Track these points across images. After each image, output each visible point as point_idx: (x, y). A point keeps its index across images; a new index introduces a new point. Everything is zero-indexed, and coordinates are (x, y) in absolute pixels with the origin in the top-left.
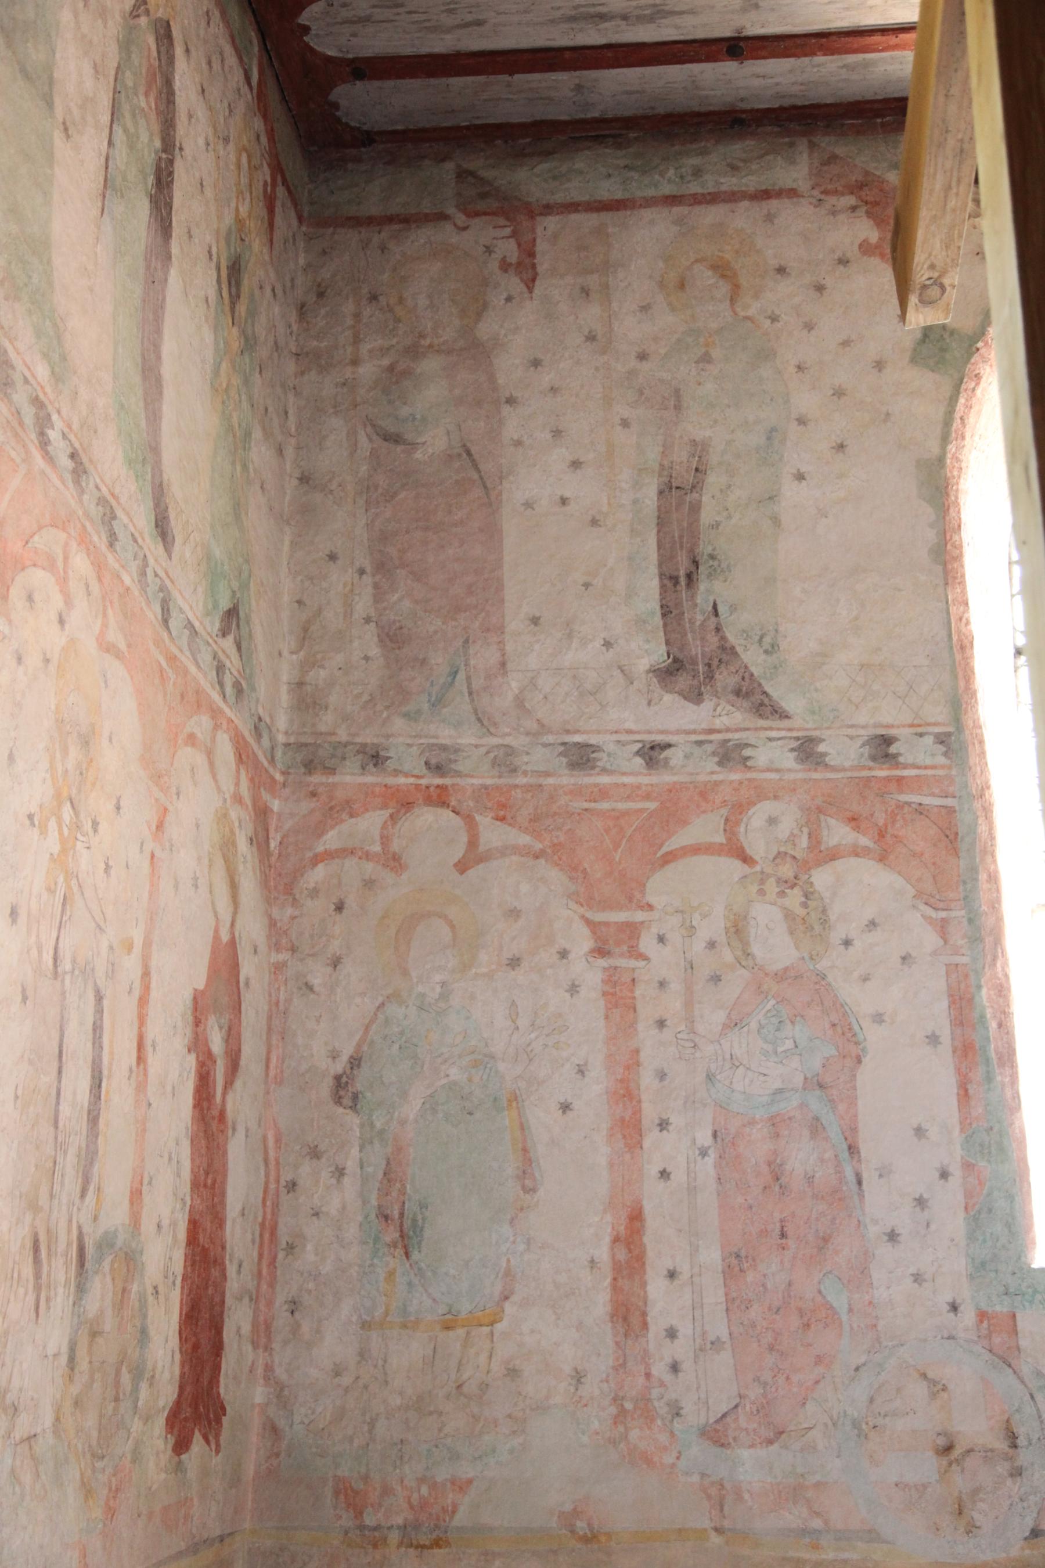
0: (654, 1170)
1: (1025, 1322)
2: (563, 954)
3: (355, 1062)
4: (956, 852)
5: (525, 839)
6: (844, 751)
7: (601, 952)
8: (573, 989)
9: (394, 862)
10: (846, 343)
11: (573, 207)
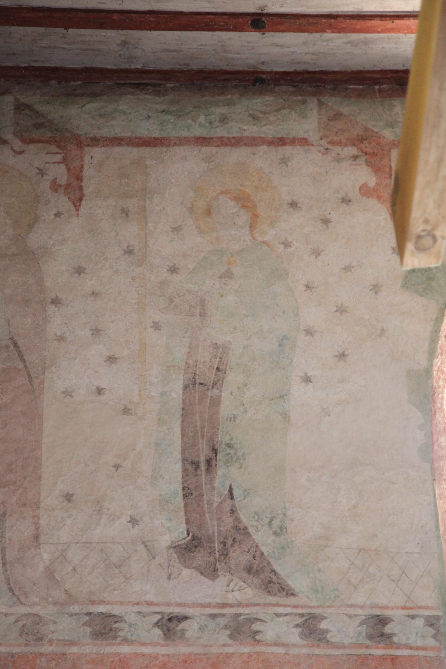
10: (347, 269)
11: (117, 141)
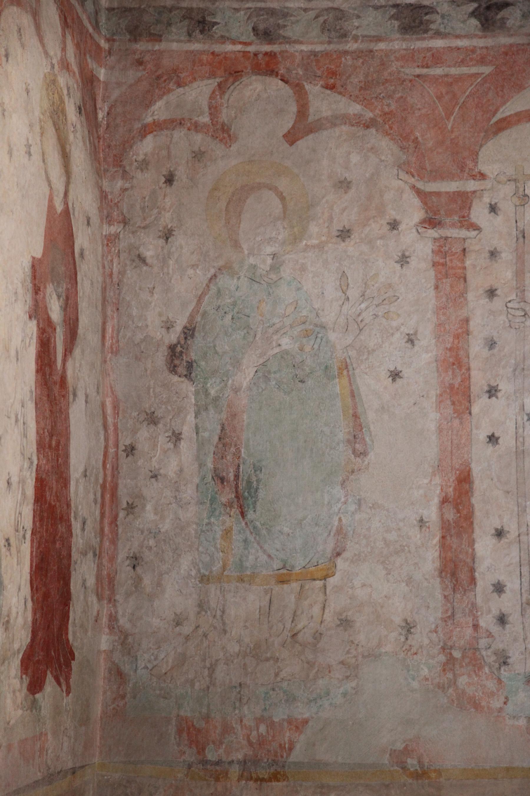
0: (482, 435)
2: (394, 225)
3: (189, 332)
5: (355, 108)
7: (431, 222)
8: (404, 260)
9: (224, 133)
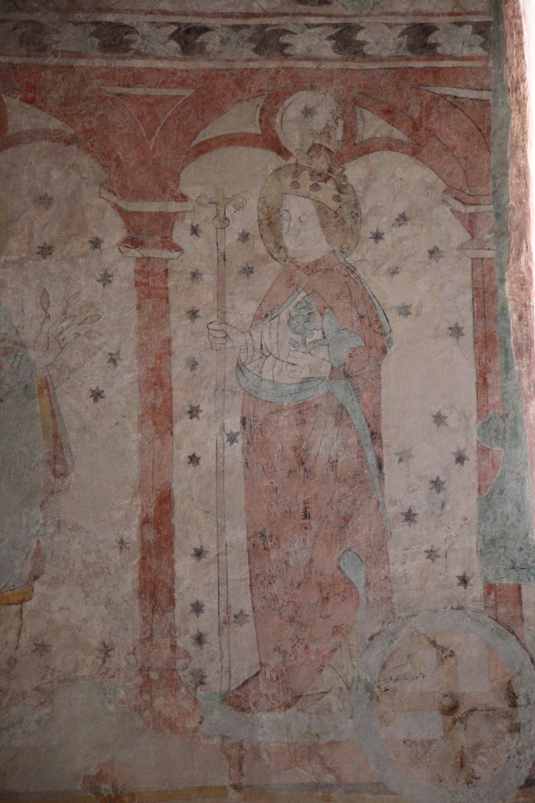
0: (183, 455)
1: (529, 594)
2: (96, 243)
4: (488, 147)
5: (55, 124)
6: (381, 39)
7: (133, 241)
8: (106, 279)
